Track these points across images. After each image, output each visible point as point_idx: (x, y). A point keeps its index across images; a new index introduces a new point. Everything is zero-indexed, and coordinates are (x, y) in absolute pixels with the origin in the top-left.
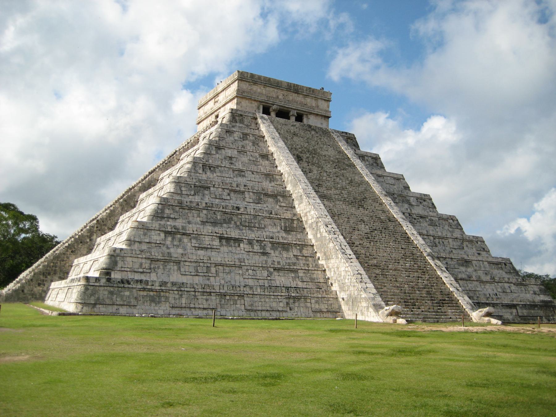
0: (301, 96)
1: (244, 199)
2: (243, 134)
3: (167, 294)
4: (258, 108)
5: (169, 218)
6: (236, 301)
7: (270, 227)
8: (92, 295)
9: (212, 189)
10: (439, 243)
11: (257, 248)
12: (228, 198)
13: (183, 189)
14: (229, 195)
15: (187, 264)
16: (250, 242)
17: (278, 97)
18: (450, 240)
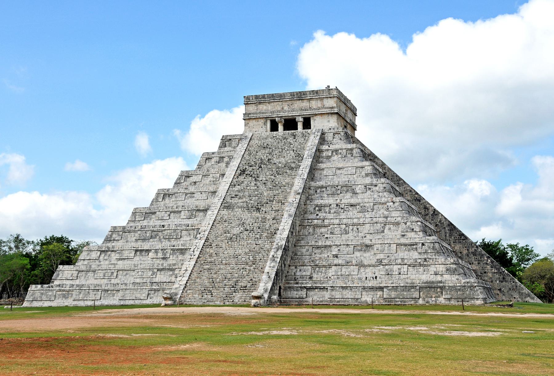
0: (305, 101)
2: (220, 158)
4: (265, 124)
6: (114, 294)
9: (157, 213)
10: (352, 230)
13: (137, 217)
15: (100, 271)
16: (156, 251)
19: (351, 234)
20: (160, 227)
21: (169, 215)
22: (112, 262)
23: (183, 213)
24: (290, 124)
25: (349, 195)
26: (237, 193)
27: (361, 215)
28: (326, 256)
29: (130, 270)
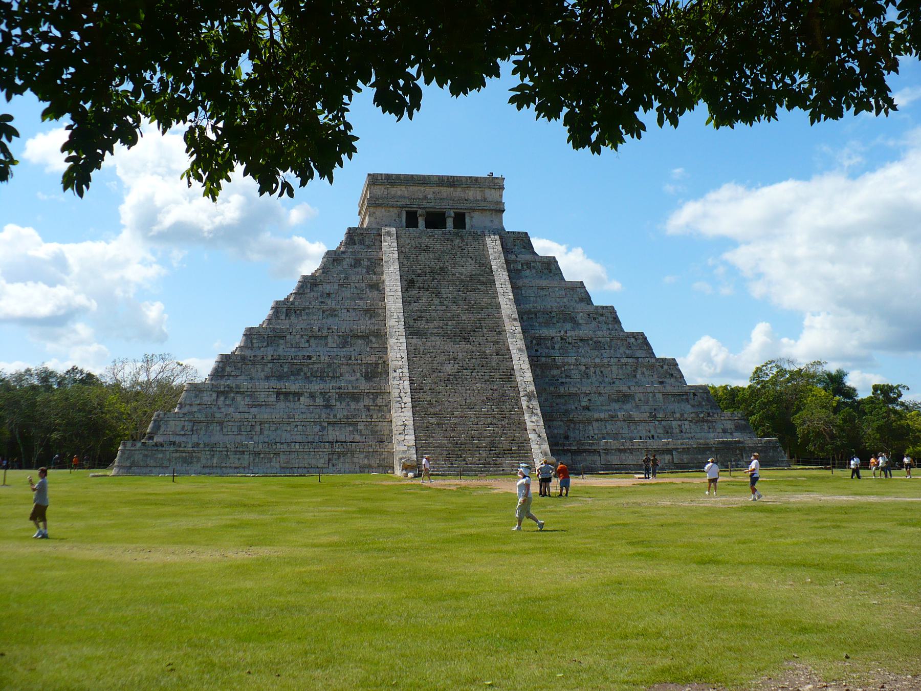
0: (459, 189)
1: (326, 344)
2: (355, 259)
3: (199, 455)
4: (399, 216)
5: (229, 375)
6: (271, 459)
7: (347, 375)
8: (128, 458)
10: (595, 373)
11: (319, 401)
12: (307, 345)
13: (255, 341)
14: (308, 341)
15: (230, 423)
16: (312, 396)
17: (425, 198)
18: (614, 368)
19: (594, 379)
20: (304, 359)
21: (308, 341)
22: (241, 410)
23: (330, 339)
24: (435, 220)
25: (568, 326)
26: (419, 314)
27: (596, 353)
28: (573, 408)
29: (282, 422)
